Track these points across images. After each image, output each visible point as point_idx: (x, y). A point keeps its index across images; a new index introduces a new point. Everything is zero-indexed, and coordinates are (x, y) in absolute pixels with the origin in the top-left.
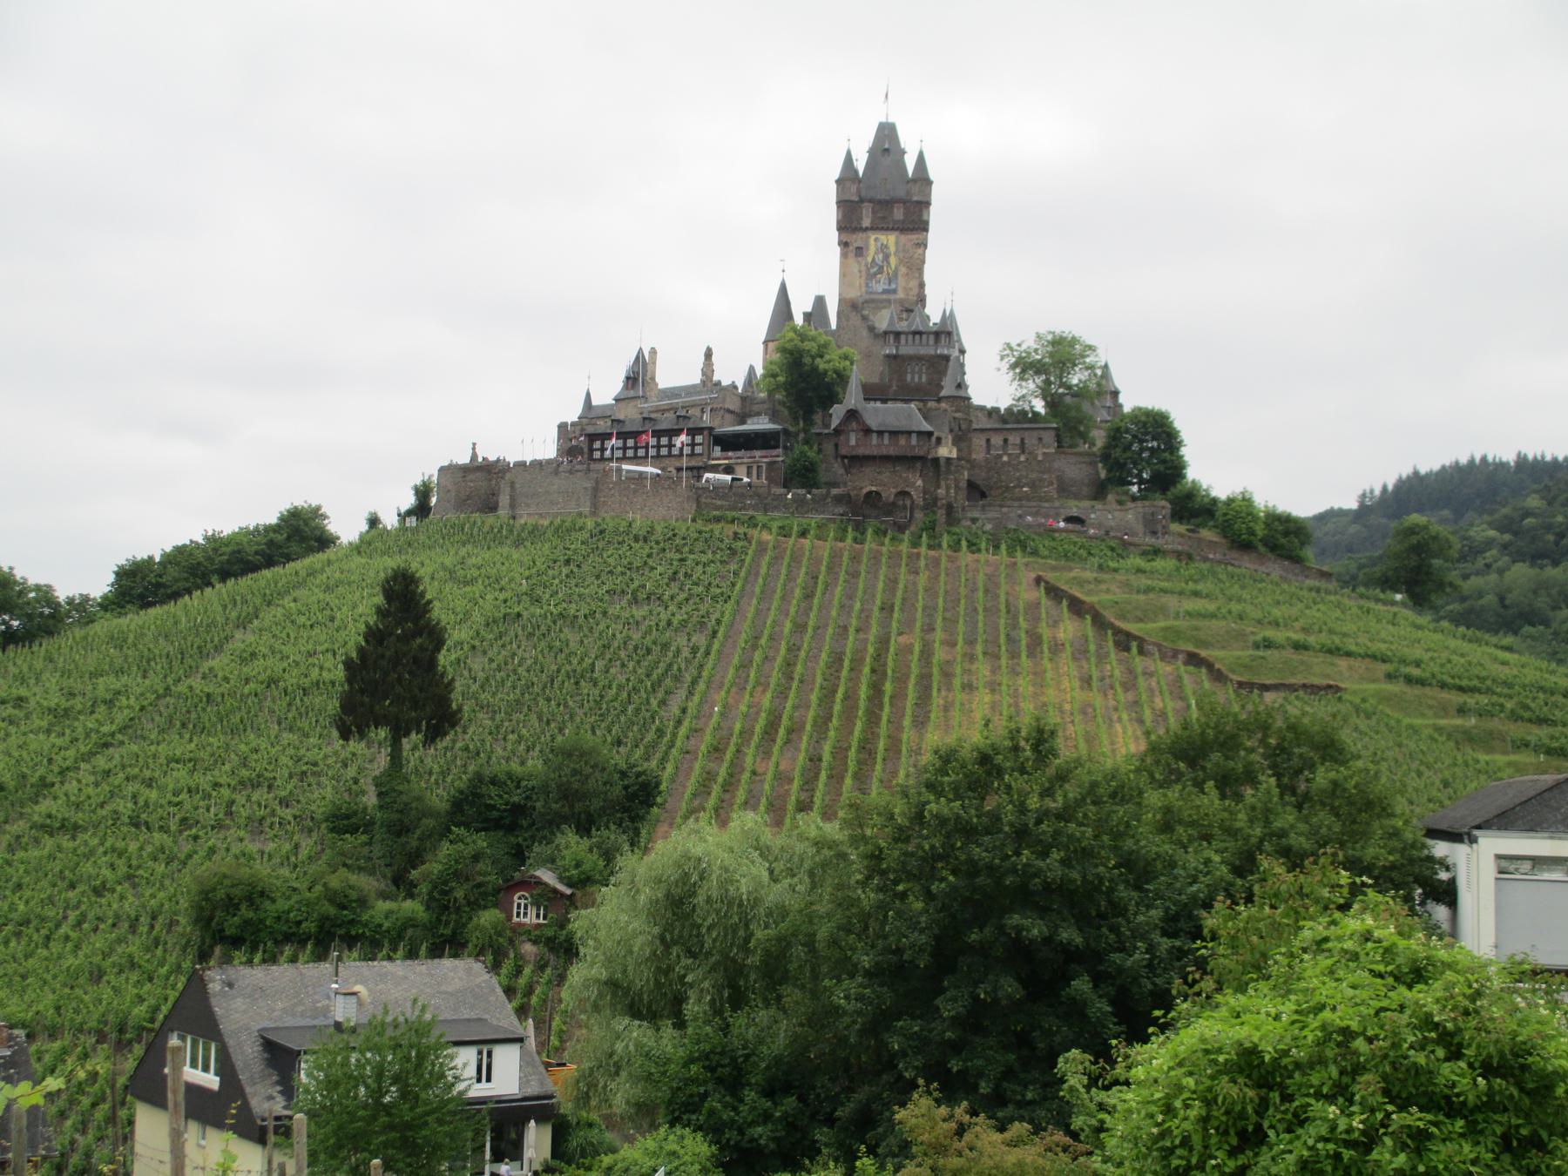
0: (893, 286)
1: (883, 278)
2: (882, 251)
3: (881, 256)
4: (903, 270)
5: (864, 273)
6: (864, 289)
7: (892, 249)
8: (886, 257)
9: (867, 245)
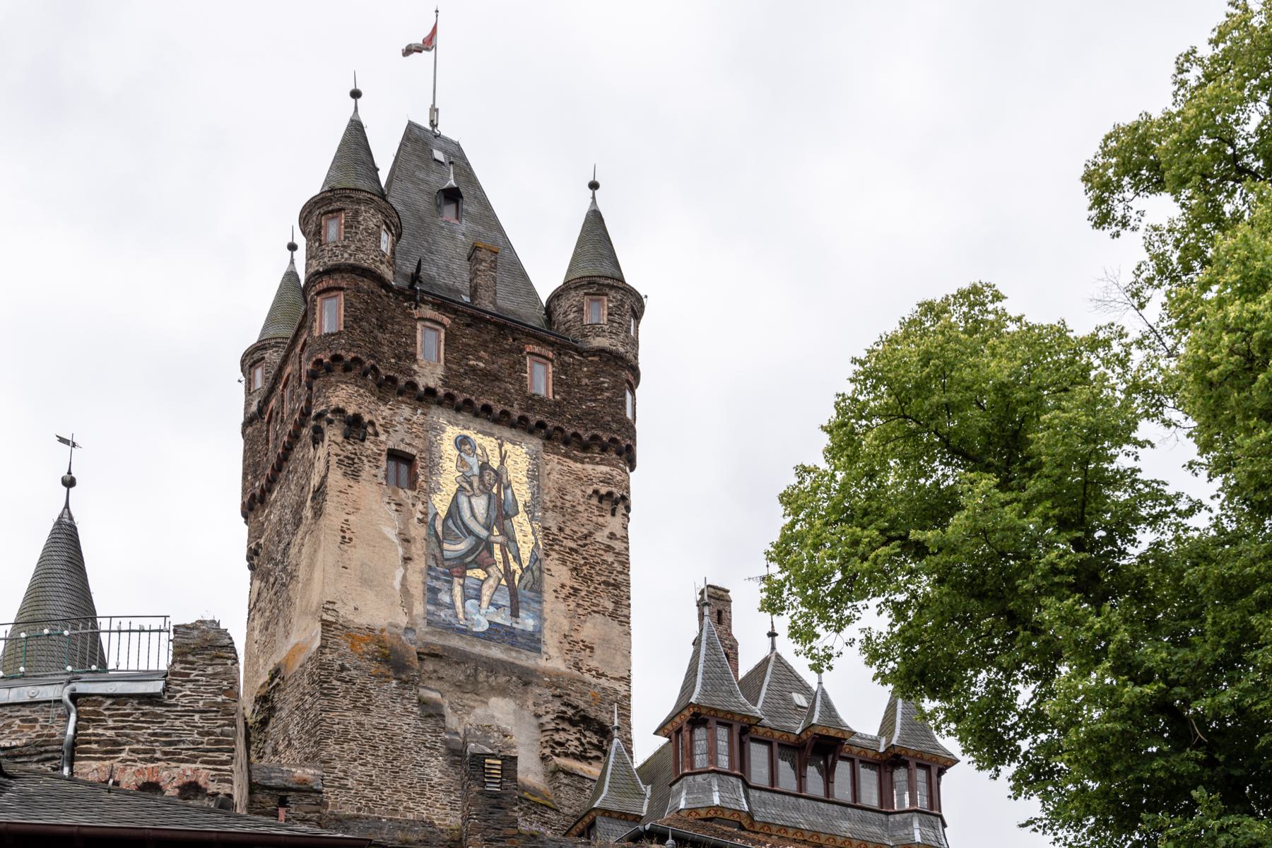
0: (527, 622)
1: (489, 580)
2: (486, 490)
3: (480, 504)
4: (559, 574)
5: (418, 550)
6: (419, 608)
7: (522, 492)
8: (501, 514)
9: (431, 449)
